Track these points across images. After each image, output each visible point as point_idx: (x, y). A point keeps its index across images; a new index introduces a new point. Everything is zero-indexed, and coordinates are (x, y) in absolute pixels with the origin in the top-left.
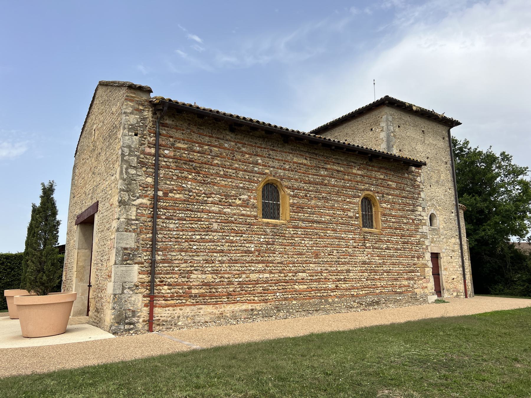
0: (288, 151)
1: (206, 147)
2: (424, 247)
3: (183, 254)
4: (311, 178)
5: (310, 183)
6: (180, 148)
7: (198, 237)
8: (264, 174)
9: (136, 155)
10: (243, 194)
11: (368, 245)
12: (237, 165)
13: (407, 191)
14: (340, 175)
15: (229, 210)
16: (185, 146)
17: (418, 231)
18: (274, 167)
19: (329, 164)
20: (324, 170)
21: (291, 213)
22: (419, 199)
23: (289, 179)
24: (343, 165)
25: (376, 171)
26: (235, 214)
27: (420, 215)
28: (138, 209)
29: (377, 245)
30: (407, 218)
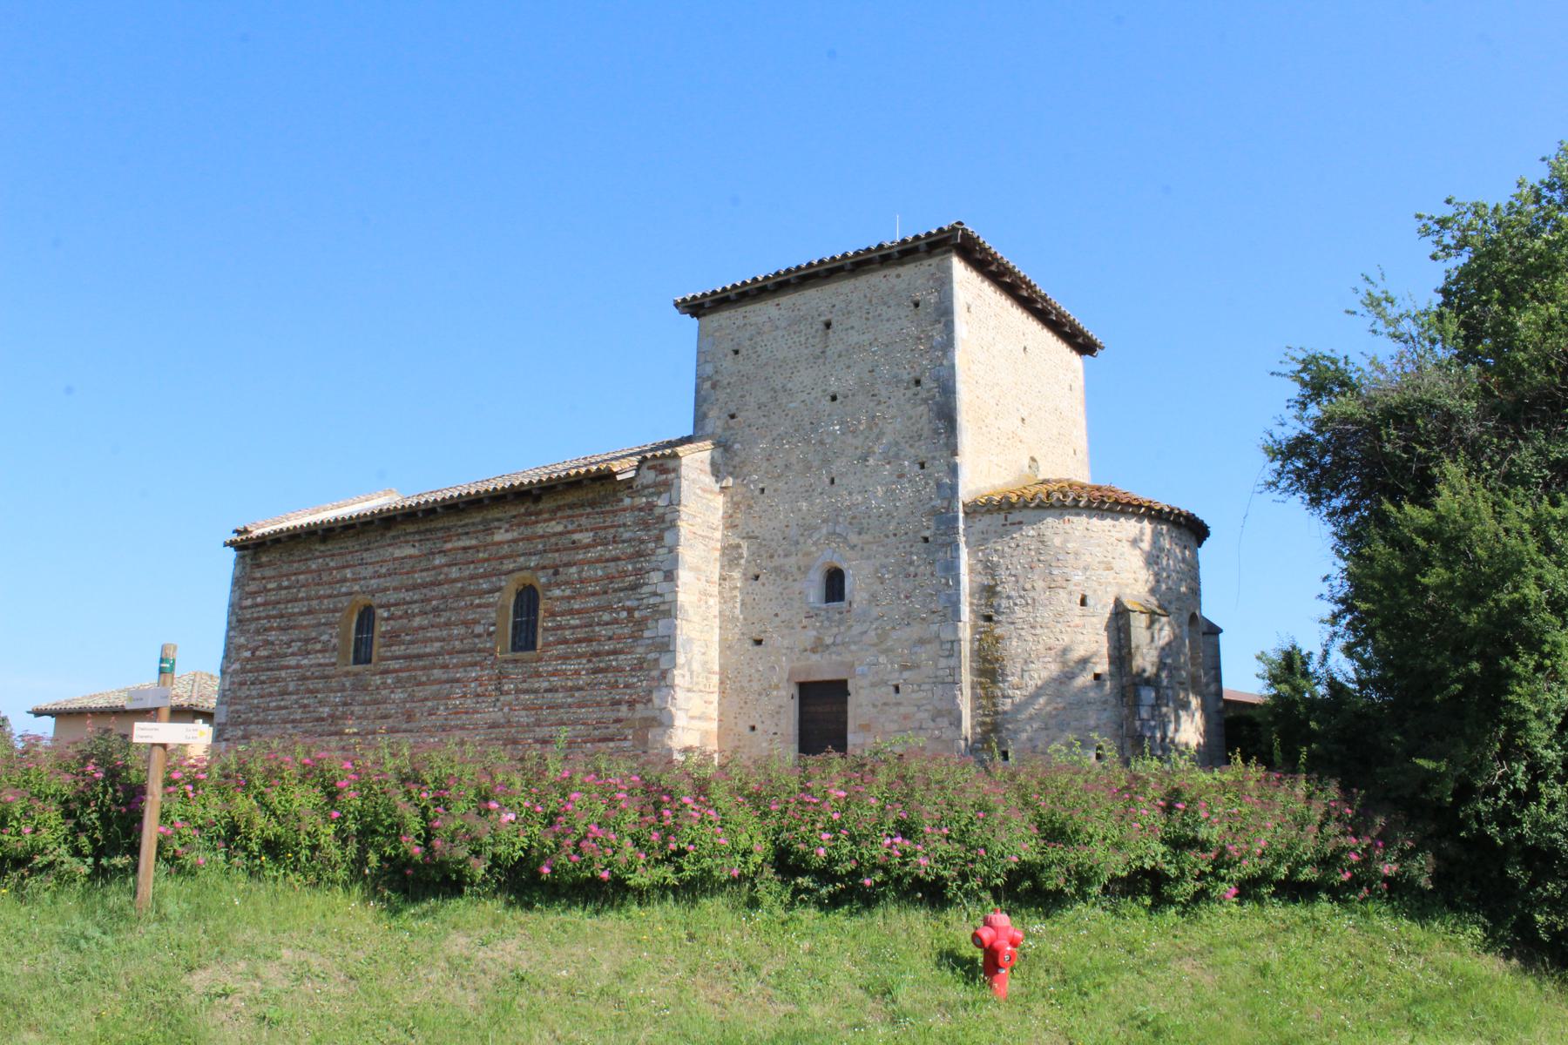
2: (655, 673)
4: (418, 578)
5: (415, 587)
14: (470, 555)
15: (305, 662)
25: (545, 521)
27: (655, 594)
29: (525, 686)
30: (613, 610)
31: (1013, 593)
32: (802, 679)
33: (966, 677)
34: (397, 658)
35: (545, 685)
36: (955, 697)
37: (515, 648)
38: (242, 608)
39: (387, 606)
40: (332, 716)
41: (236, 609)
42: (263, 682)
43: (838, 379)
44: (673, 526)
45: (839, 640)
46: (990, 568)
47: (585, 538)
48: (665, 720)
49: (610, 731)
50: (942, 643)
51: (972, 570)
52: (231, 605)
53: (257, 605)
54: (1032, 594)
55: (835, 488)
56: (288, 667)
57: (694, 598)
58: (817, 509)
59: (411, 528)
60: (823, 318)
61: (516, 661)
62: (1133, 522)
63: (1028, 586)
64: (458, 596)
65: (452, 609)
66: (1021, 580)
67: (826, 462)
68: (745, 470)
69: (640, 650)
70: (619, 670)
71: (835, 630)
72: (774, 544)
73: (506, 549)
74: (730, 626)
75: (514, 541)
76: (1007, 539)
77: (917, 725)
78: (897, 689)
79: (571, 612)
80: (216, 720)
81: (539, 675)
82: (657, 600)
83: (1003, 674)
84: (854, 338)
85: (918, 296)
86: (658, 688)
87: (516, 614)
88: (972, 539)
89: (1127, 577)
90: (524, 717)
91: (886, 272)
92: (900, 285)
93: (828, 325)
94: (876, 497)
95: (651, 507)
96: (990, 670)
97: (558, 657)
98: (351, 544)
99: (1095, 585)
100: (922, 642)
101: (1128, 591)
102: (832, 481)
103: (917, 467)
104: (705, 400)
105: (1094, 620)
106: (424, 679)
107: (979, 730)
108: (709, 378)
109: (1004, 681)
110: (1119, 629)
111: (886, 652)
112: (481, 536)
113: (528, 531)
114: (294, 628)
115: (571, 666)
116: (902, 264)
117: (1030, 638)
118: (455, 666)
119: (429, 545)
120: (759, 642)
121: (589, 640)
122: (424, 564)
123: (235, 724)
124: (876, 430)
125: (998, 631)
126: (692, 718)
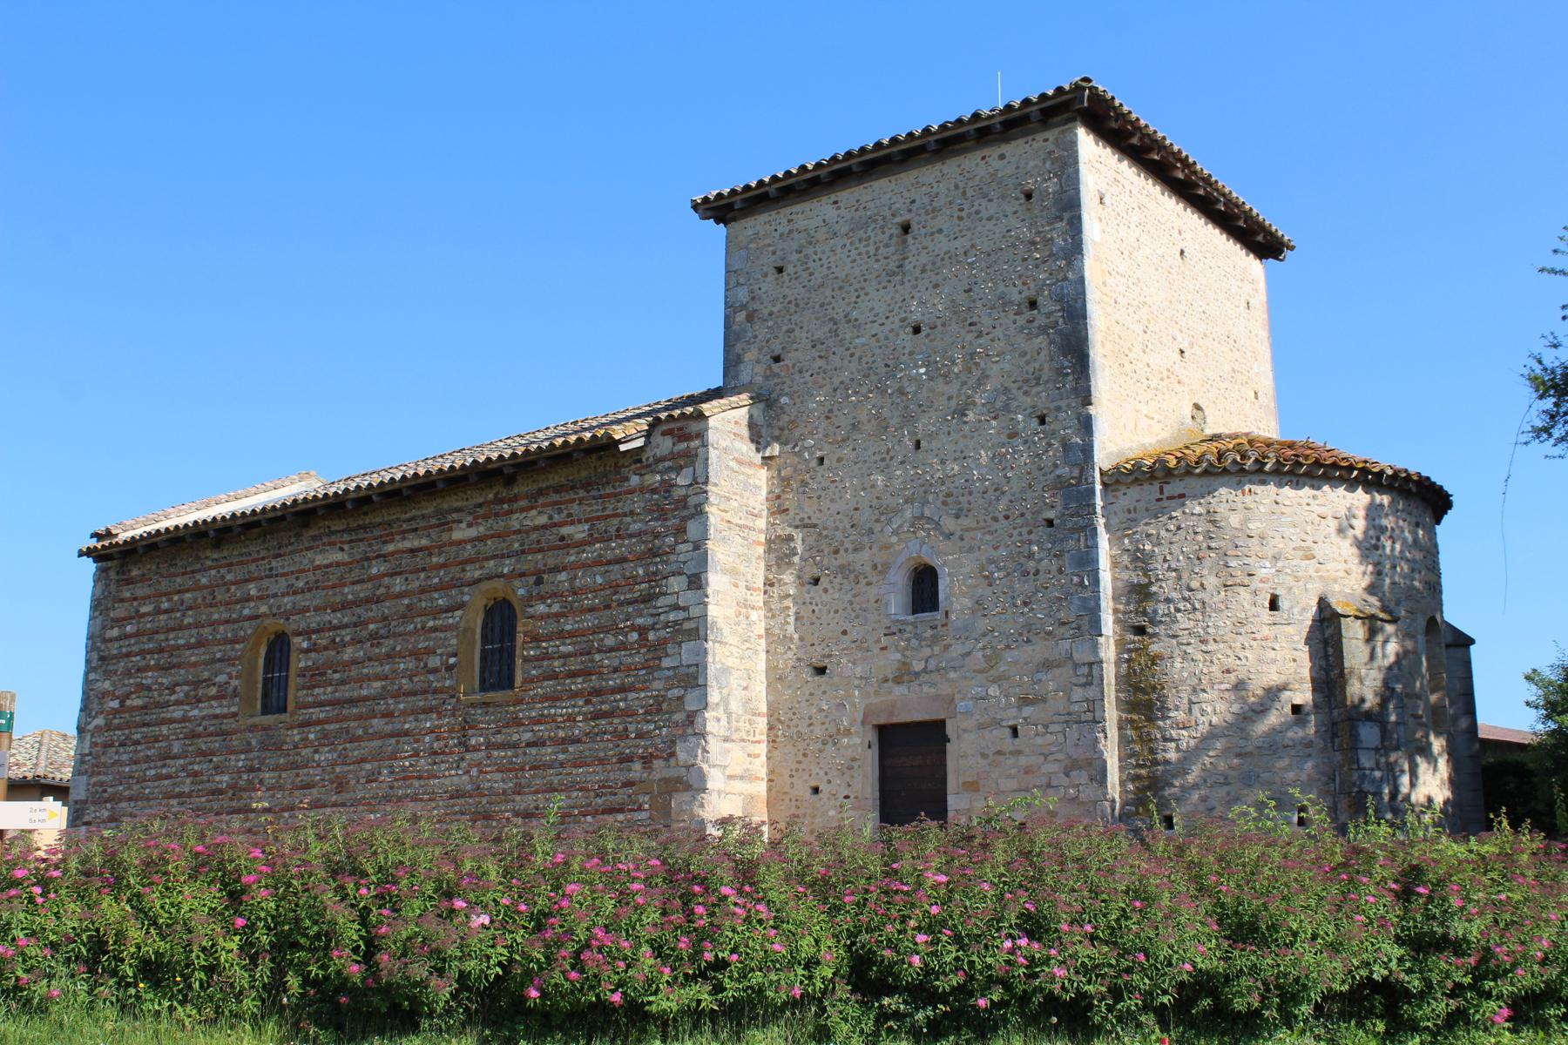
1: (176, 598)
5: (345, 606)
7: (153, 772)
12: (216, 616)
13: (631, 536)
14: (420, 559)
15: (195, 712)
17: (659, 668)
19: (392, 541)
21: (300, 693)
23: (306, 610)
24: (425, 528)
25: (522, 510)
26: (203, 718)
27: (676, 607)
29: (499, 738)
31: (1174, 595)
32: (882, 721)
33: (1111, 714)
34: (321, 704)
35: (527, 736)
36: (1096, 740)
37: (485, 686)
38: (105, 641)
39: (306, 633)
40: (232, 787)
41: (96, 641)
42: (137, 743)
43: (921, 303)
44: (699, 513)
45: (932, 664)
46: (1140, 560)
47: (578, 532)
48: (693, 781)
49: (619, 798)
50: (1076, 666)
51: (1115, 564)
52: (91, 637)
53: (127, 636)
54: (1200, 595)
55: (921, 455)
56: (171, 721)
57: (731, 612)
58: (897, 484)
59: (338, 525)
60: (898, 220)
61: (486, 704)
62: (1341, 491)
63: (1195, 584)
64: (405, 617)
65: (396, 635)
66: (1185, 575)
67: (908, 419)
68: (797, 434)
69: (658, 685)
70: (628, 713)
71: (927, 652)
72: (839, 534)
74: (781, 649)
75: (480, 539)
76: (1164, 519)
77: (1044, 781)
78: (1015, 732)
79: (561, 635)
80: (73, 796)
81: (518, 723)
82: (681, 615)
83: (1164, 708)
84: (942, 245)
85: (1030, 184)
86: (684, 737)
87: (483, 645)
88: (1114, 521)
89: (1334, 568)
90: (497, 781)
91: (985, 152)
92: (1005, 169)
93: (906, 228)
94: (979, 466)
95: (668, 487)
96: (1144, 701)
97: (545, 698)
98: (255, 549)
99: (1289, 580)
100: (1047, 665)
101: (1337, 588)
102: (918, 445)
103: (1035, 423)
104: (738, 338)
105: (1290, 629)
106: (360, 732)
107: (1131, 787)
108: (743, 307)
109: (1164, 718)
110: (1325, 642)
111: (997, 680)
112: (433, 533)
113: (500, 525)
114: (179, 666)
116: (1007, 140)
117: (1199, 656)
118: (403, 713)
119: (362, 547)
120: (821, 671)
121: (586, 673)
122: (356, 574)
123: (99, 802)
124: (976, 373)
125: (1155, 648)
126: (731, 777)
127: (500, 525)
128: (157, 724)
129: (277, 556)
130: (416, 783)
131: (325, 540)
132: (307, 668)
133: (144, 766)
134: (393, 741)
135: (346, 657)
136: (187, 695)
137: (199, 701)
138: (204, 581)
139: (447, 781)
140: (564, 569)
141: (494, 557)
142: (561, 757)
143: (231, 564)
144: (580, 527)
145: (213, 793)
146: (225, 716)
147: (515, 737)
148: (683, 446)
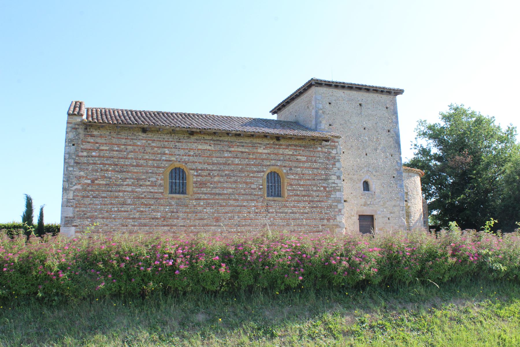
0: (193, 141)
1: (123, 147)
2: (336, 210)
3: (105, 220)
4: (215, 160)
5: (213, 164)
6: (103, 150)
8: (170, 161)
9: (73, 158)
10: (152, 177)
11: (271, 211)
12: (147, 157)
13: (320, 163)
15: (140, 190)
16: (107, 148)
17: (330, 197)
18: (179, 155)
19: (233, 147)
20: (228, 152)
21: (195, 189)
22: (334, 169)
23: (194, 162)
24: (248, 146)
25: (283, 149)
26: (144, 192)
27: (334, 183)
28: (74, 192)
32: (361, 214)
34: (206, 194)
35: (291, 211)
38: (78, 156)
39: (197, 170)
40: (164, 218)
45: (372, 203)
47: (304, 159)
55: (367, 157)
56: (125, 191)
64: (241, 171)
65: (237, 176)
69: (330, 201)
70: (320, 207)
71: (371, 200)
72: (349, 171)
73: (264, 156)
75: (269, 154)
78: (389, 219)
79: (300, 185)
82: (335, 185)
100: (395, 206)
102: (366, 155)
106: (224, 204)
108: (321, 109)
112: (250, 149)
113: (276, 151)
114: (128, 172)
115: (301, 205)
118: (242, 200)
119: (219, 147)
121: (309, 196)
122: (218, 155)
125: (409, 205)
127: (276, 151)
128: (116, 192)
129: (179, 142)
130: (250, 221)
131: (202, 141)
132: (197, 181)
133: (110, 207)
134: (239, 208)
135: (215, 180)
136: (133, 183)
137: (141, 186)
138: (139, 143)
139: (262, 221)
140: (299, 167)
141: (274, 160)
142: (302, 217)
143: (154, 140)
144: (303, 157)
145: (153, 219)
146: (156, 193)
147: (286, 211)
148: (333, 144)
